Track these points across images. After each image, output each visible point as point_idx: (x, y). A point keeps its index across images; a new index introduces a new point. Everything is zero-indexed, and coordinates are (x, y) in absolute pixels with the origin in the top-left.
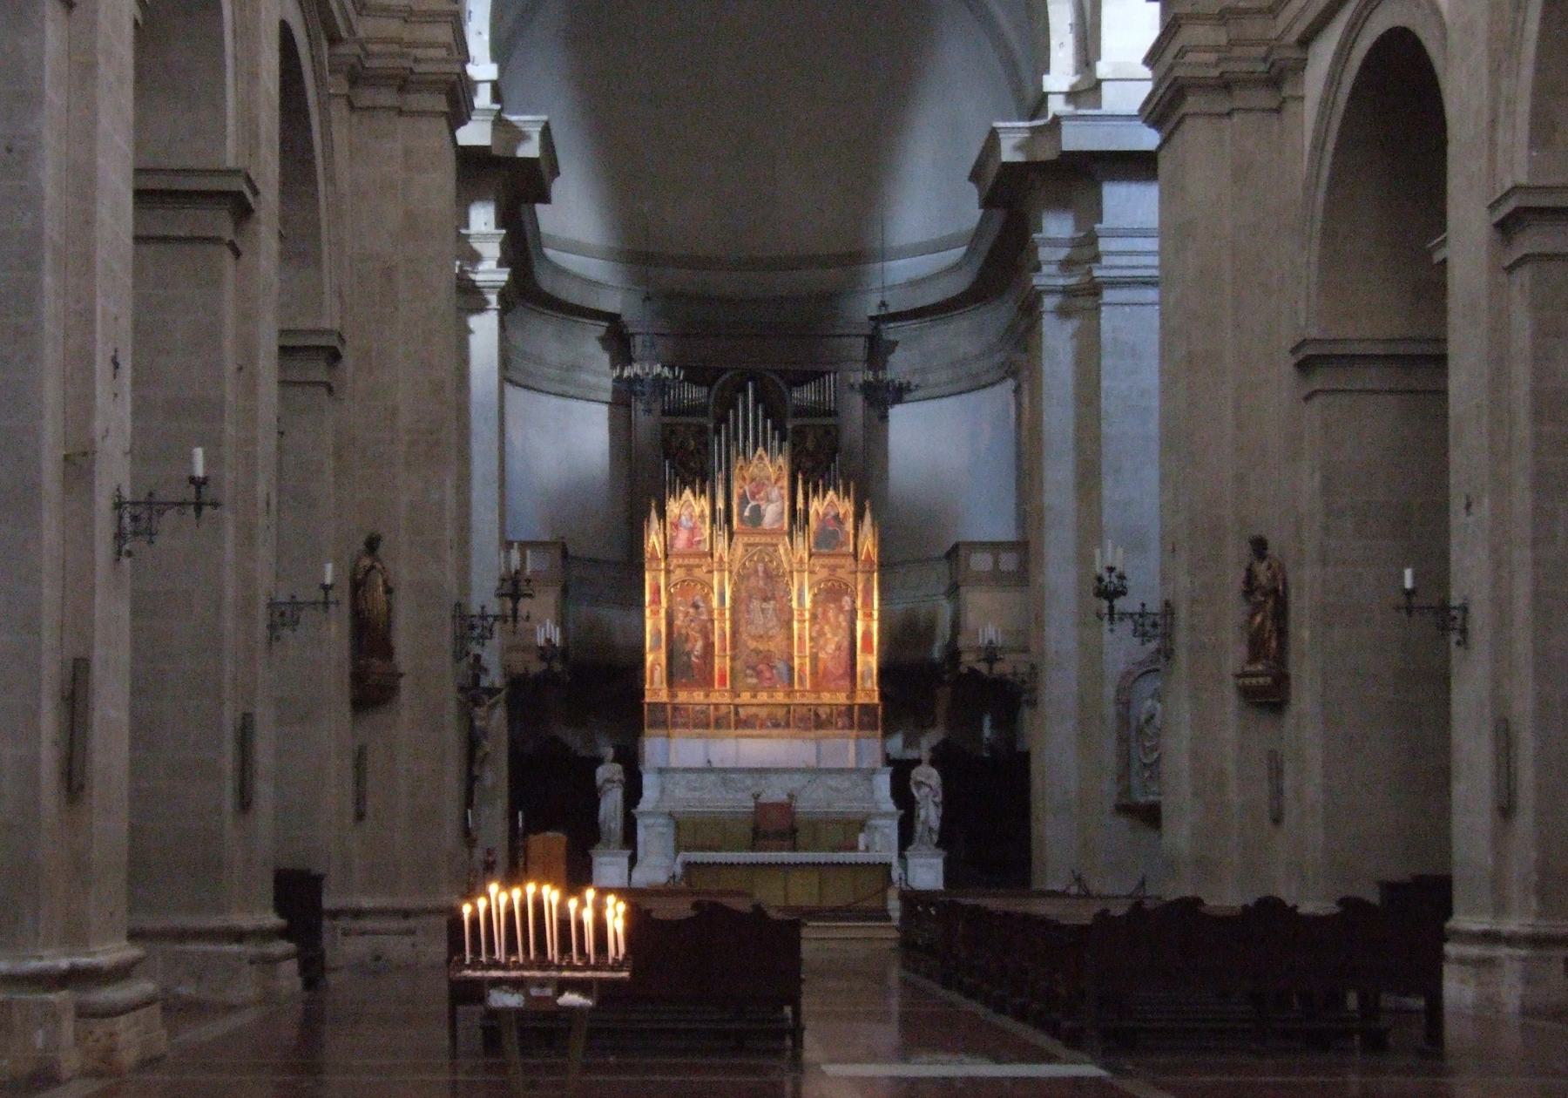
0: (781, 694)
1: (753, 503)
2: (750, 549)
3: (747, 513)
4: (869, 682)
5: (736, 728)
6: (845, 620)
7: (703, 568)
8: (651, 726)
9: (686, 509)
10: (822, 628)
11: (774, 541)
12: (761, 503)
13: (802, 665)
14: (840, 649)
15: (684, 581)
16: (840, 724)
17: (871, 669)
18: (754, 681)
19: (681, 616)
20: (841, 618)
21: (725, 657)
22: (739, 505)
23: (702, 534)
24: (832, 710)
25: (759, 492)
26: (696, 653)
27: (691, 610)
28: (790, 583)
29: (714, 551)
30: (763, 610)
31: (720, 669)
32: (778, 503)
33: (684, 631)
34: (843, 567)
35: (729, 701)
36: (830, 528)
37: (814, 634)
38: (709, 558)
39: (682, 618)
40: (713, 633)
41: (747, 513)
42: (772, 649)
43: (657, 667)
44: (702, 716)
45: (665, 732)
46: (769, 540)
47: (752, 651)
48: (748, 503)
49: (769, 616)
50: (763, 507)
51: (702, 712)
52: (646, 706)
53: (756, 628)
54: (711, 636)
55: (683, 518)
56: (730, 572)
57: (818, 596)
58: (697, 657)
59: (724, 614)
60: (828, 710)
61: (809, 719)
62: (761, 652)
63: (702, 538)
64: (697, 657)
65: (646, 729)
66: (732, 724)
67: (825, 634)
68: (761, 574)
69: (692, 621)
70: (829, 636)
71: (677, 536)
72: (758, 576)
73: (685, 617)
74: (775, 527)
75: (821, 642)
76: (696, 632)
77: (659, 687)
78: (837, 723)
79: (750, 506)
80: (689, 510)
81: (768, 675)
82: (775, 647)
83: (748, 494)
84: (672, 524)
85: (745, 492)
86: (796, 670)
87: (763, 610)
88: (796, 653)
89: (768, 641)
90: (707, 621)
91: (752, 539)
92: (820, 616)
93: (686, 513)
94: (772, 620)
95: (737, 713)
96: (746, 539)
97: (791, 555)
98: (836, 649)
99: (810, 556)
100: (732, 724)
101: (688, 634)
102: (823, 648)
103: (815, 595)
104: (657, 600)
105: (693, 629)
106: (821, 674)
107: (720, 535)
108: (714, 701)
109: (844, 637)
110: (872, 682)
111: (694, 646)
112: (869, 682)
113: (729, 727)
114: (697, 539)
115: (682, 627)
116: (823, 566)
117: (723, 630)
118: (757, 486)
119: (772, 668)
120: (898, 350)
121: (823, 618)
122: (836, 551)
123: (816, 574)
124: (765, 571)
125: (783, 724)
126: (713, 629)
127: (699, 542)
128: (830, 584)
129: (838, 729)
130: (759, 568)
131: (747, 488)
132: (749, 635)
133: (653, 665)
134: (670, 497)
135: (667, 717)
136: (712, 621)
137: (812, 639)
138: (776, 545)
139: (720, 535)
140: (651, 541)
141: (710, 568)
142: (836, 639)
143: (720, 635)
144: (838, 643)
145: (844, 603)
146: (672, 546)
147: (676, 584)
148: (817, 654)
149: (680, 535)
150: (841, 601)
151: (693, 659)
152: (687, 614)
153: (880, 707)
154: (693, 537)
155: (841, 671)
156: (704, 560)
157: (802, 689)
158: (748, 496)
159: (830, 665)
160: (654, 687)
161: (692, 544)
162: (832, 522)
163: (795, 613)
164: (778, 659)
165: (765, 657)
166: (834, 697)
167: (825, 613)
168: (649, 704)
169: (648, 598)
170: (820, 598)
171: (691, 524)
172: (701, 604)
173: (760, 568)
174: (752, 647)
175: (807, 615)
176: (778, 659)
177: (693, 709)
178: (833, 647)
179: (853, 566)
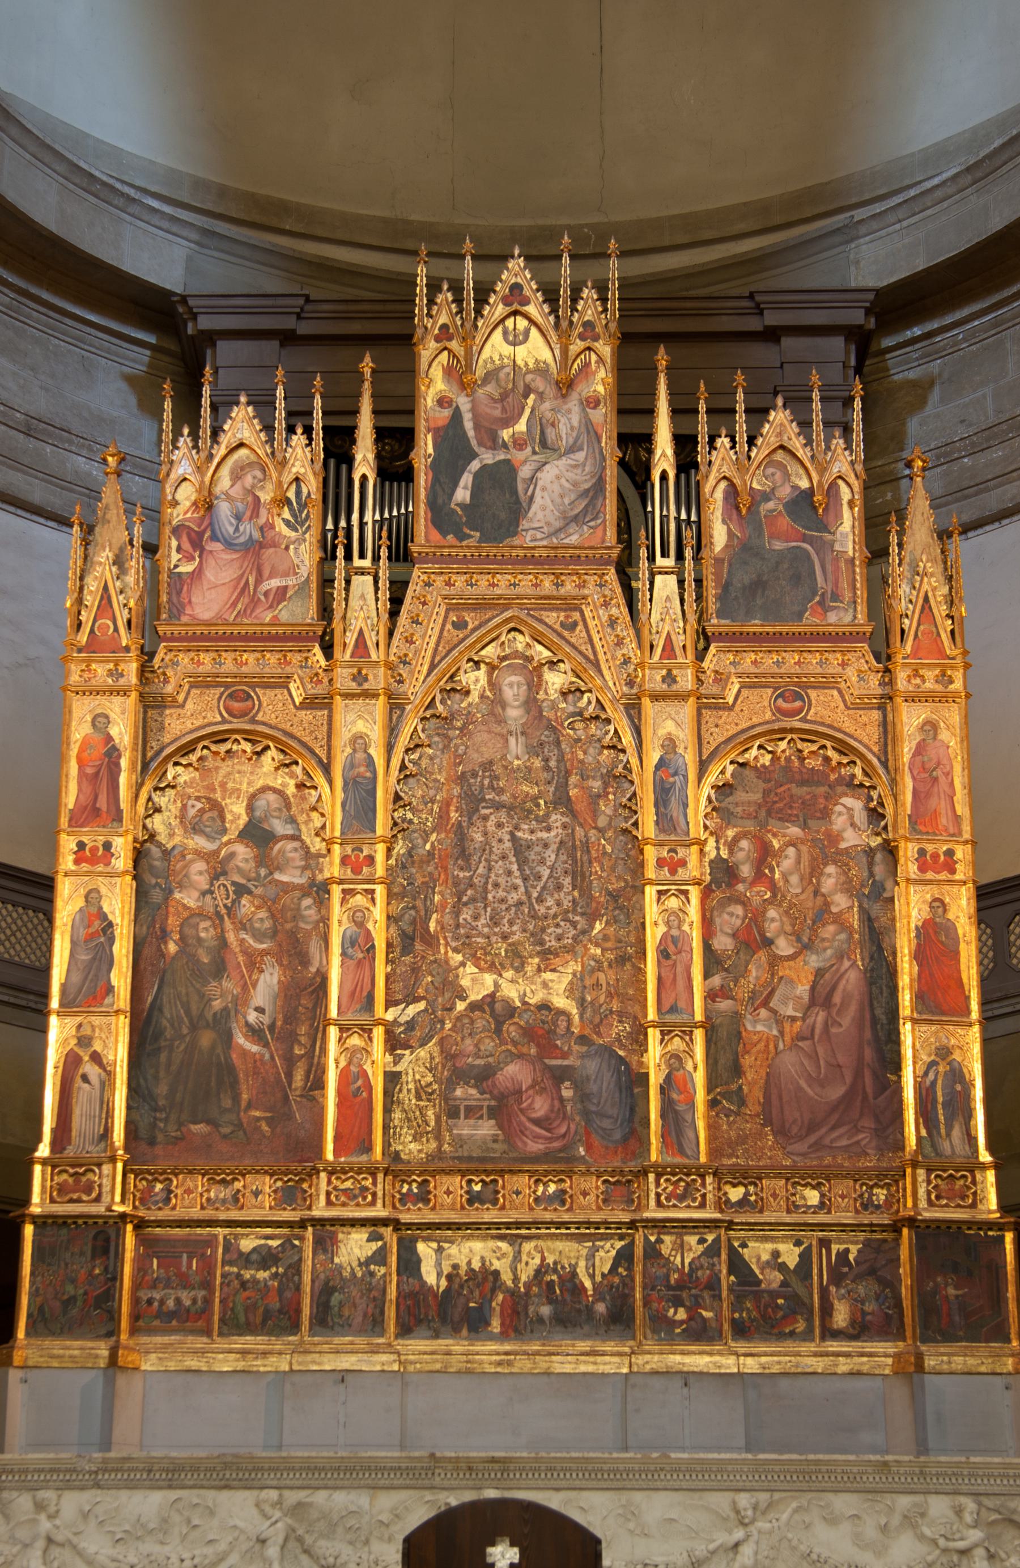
0: (594, 1185)
1: (488, 457)
2: (471, 619)
3: (462, 494)
4: (957, 1132)
5: (405, 1330)
6: (847, 887)
7: (292, 686)
8: (40, 1325)
9: (236, 476)
10: (756, 918)
11: (569, 587)
12: (518, 456)
13: (675, 1061)
14: (827, 1003)
15: (219, 738)
16: (841, 1317)
17: (957, 1076)
18: (486, 1129)
19: (198, 872)
20: (831, 878)
21: (367, 1031)
22: (435, 466)
23: (293, 570)
24: (805, 1257)
25: (509, 421)
26: (252, 1017)
27: (242, 851)
28: (628, 739)
29: (337, 624)
30: (520, 849)
31: (345, 1078)
32: (580, 456)
33: (206, 931)
34: (827, 683)
35: (379, 1211)
36: (778, 545)
37: (723, 943)
38: (318, 655)
39: (202, 881)
40: (326, 939)
41: (462, 494)
42: (561, 1002)
43: (90, 1069)
44: (262, 1275)
45: (102, 1350)
46: (547, 585)
47: (474, 1007)
48: (474, 455)
49: (546, 873)
50: (525, 472)
51: (265, 1258)
52: (29, 1230)
53: (495, 921)
54: (314, 948)
55: (224, 509)
56: (396, 705)
57: (740, 796)
58: (255, 1033)
59: (371, 860)
60: (790, 1255)
61: (713, 1285)
62: (511, 1011)
63: (291, 581)
64: (255, 1033)
65: (21, 1333)
66: (391, 1313)
67: (769, 943)
68: (514, 713)
69: (241, 890)
70: (784, 947)
71: (197, 574)
72: (501, 721)
73: (215, 877)
74: (574, 539)
75: (756, 972)
76: (258, 936)
77: (95, 1151)
78: (827, 1310)
79: (475, 465)
80: (248, 480)
81: (540, 1106)
82: (570, 991)
83: (468, 425)
84: (176, 531)
85: (457, 416)
86: (655, 1080)
87: (520, 849)
88: (652, 1015)
89: (539, 970)
90: (305, 891)
91: (483, 581)
92: (746, 871)
93: (236, 491)
94: (559, 887)
95: (409, 1264)
96: (460, 581)
97: (630, 647)
98: (813, 1002)
99: (705, 638)
100: (391, 1313)
101: (223, 943)
102: (763, 999)
103: (723, 789)
104: (102, 803)
105: (242, 926)
106: (755, 1095)
107: (362, 572)
108: (320, 1210)
109: (840, 956)
110: (972, 1140)
111: (247, 988)
112: (957, 1132)
113: (375, 1324)
114: (275, 583)
115: (200, 914)
116: (752, 683)
117: (359, 918)
118: (504, 396)
119: (559, 1076)
120: (935, 396)
121: (759, 876)
122: (811, 621)
123: (731, 708)
124: (531, 704)
125: (601, 1308)
126: (325, 920)
127: (281, 593)
128: (783, 745)
129: (836, 1334)
130: (508, 693)
131: (463, 403)
132: (466, 945)
133: (71, 1063)
134: (177, 433)
135: (114, 1277)
136: (320, 890)
137: (712, 961)
138: (571, 605)
139: (362, 572)
140: (92, 585)
141: (320, 690)
142: (814, 961)
143: (349, 943)
144: (819, 973)
145: (839, 822)
146: (177, 611)
147: (188, 749)
148: (736, 1018)
149: (209, 574)
150: (826, 814)
151: (240, 1040)
152: (219, 868)
153: (1009, 1237)
154: (258, 582)
155: (836, 1092)
156: (296, 658)
157: (678, 1160)
158: (471, 433)
159: (789, 1062)
160: (70, 1151)
161: (255, 602)
162: (785, 522)
163: (651, 854)
164: (583, 1039)
165: (529, 1033)
166: (813, 1197)
167: (764, 854)
168: (41, 1222)
169: (70, 797)
170: (749, 796)
171: (248, 529)
172: (280, 827)
173: (513, 686)
174: (475, 996)
175: (695, 867)
176: (583, 1039)
177: (227, 1248)
178: (803, 989)
179: (874, 683)
